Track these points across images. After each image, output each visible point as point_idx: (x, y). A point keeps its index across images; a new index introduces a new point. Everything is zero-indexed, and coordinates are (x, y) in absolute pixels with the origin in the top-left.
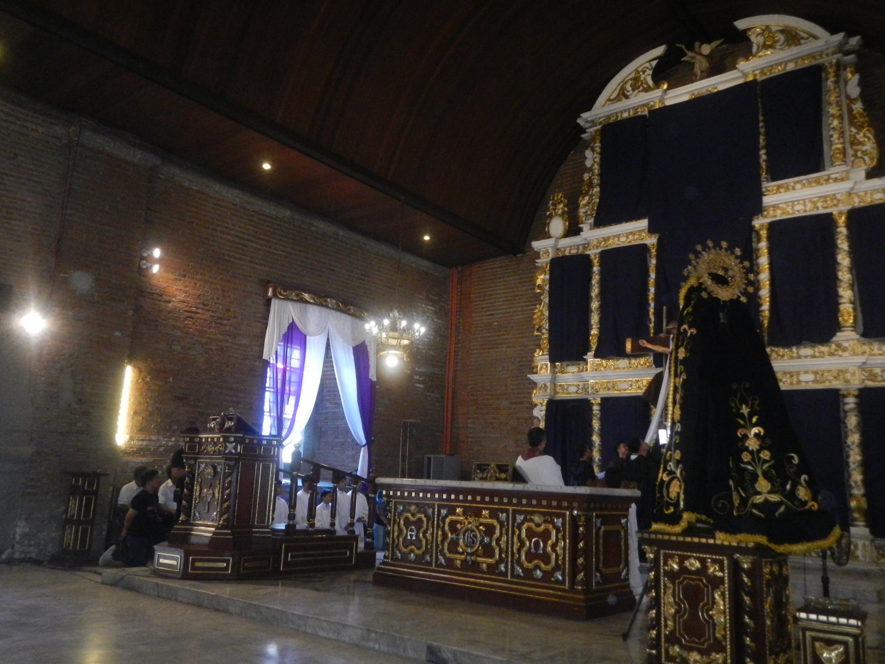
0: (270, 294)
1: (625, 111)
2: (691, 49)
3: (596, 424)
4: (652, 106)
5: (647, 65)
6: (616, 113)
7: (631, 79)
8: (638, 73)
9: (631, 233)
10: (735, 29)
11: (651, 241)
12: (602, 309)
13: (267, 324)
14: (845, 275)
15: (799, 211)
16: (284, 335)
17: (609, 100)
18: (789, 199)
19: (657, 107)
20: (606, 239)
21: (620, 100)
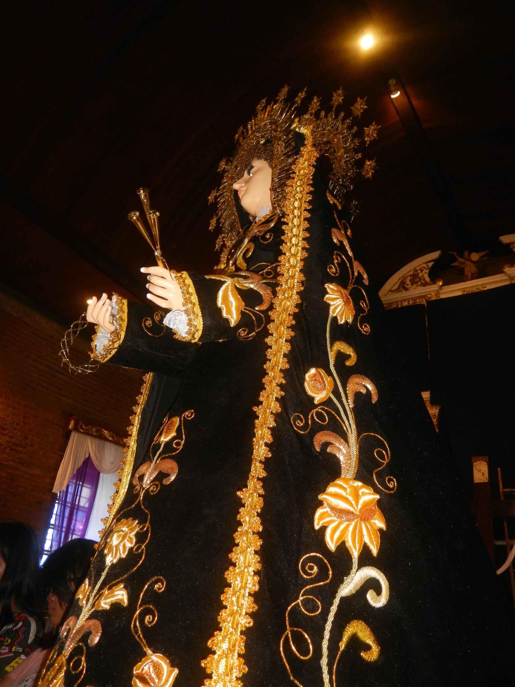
0: (70, 427)
1: (405, 300)
2: (462, 256)
4: (429, 298)
5: (425, 265)
6: (397, 302)
7: (410, 276)
8: (417, 271)
10: (501, 243)
13: (62, 457)
16: (79, 470)
17: (391, 291)
19: (434, 299)
21: (401, 291)
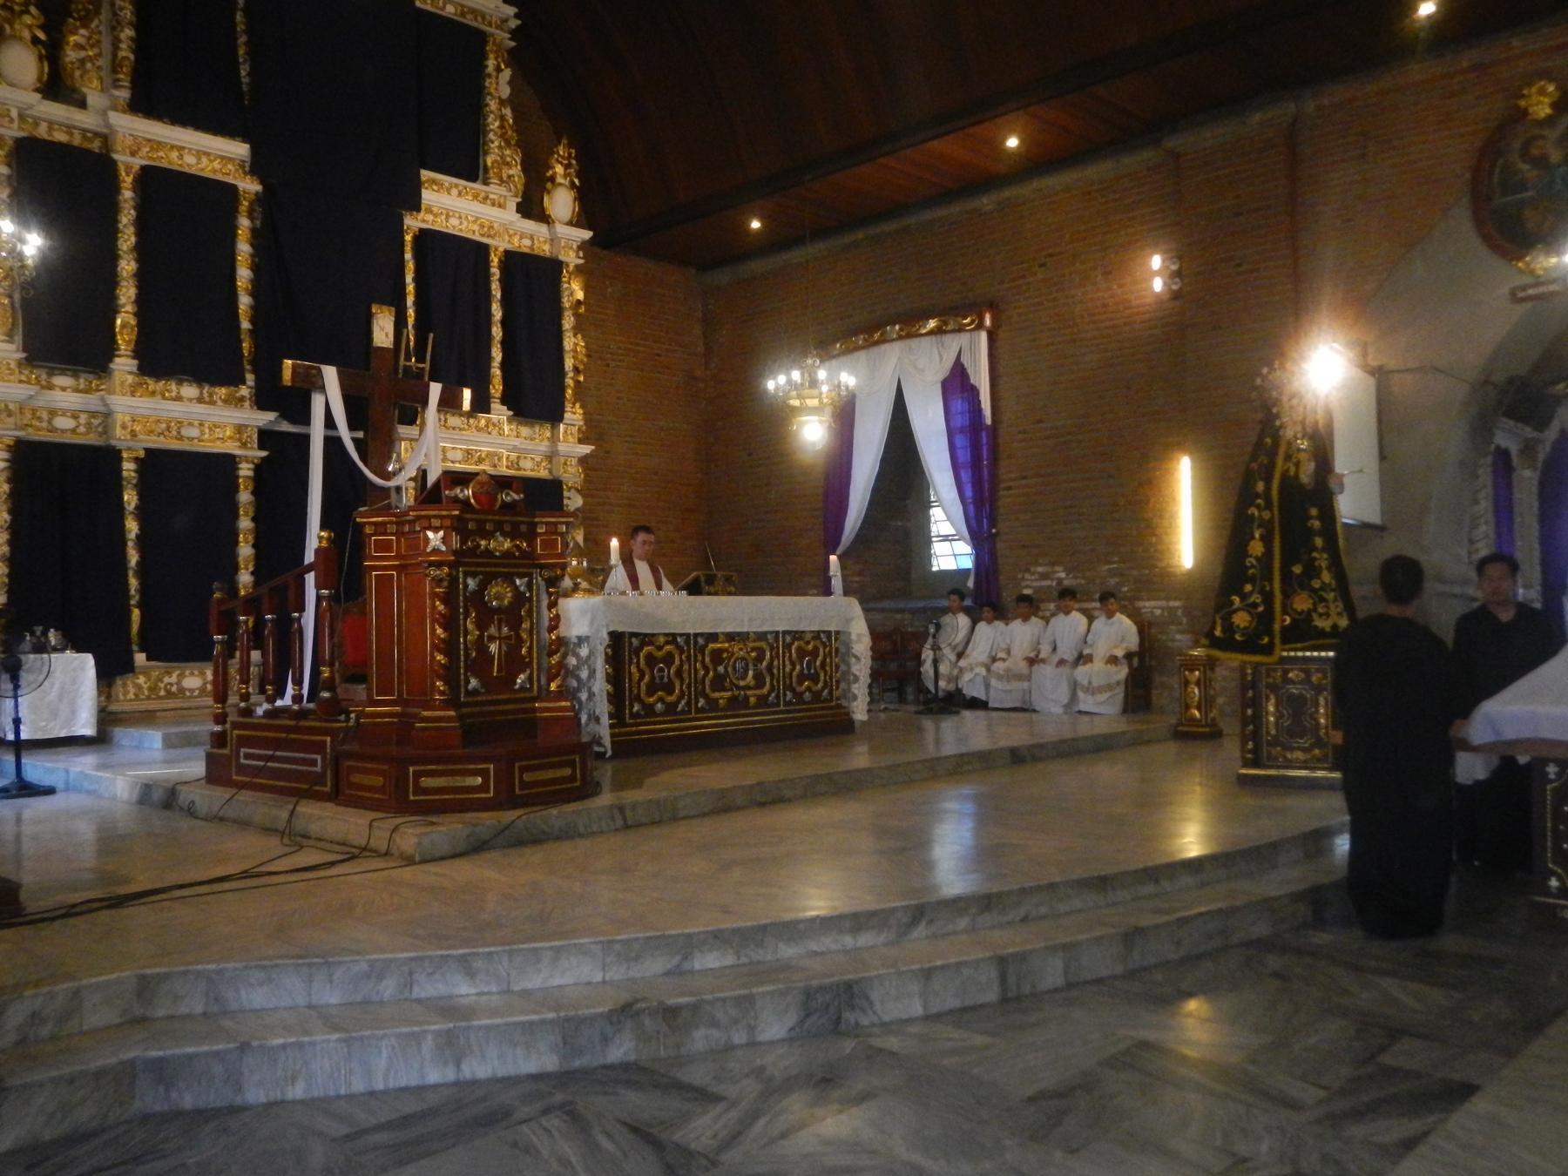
3: (130, 498)
9: (207, 154)
11: (250, 186)
12: (141, 277)
14: (497, 332)
15: (453, 226)
18: (449, 206)
20: (157, 145)
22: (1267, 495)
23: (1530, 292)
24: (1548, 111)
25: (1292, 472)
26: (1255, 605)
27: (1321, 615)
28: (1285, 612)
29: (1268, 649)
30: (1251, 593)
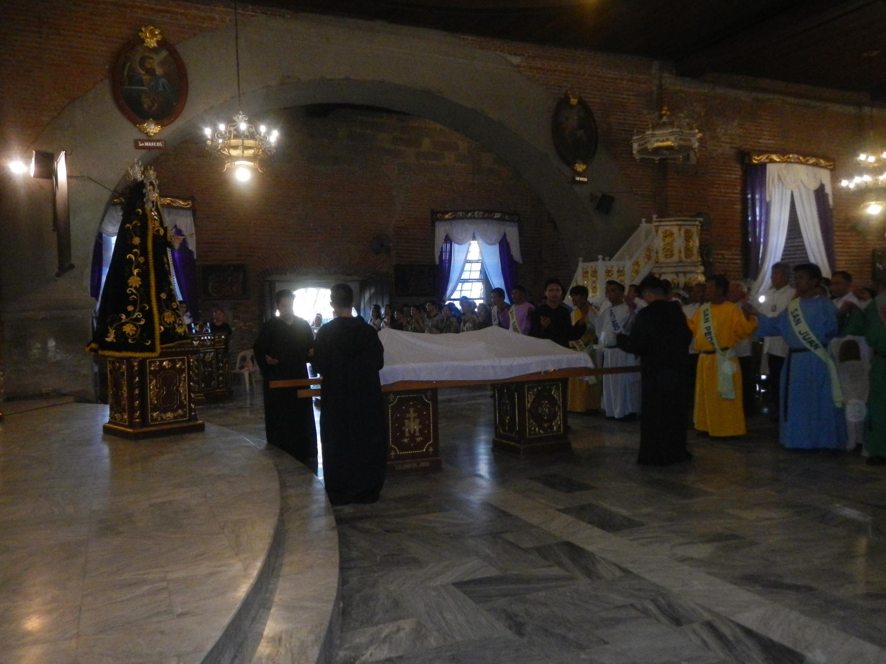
22: (143, 247)
23: (147, 144)
24: (155, 45)
25: (162, 232)
26: (139, 320)
27: (179, 325)
28: (161, 324)
29: (152, 349)
30: (134, 311)
